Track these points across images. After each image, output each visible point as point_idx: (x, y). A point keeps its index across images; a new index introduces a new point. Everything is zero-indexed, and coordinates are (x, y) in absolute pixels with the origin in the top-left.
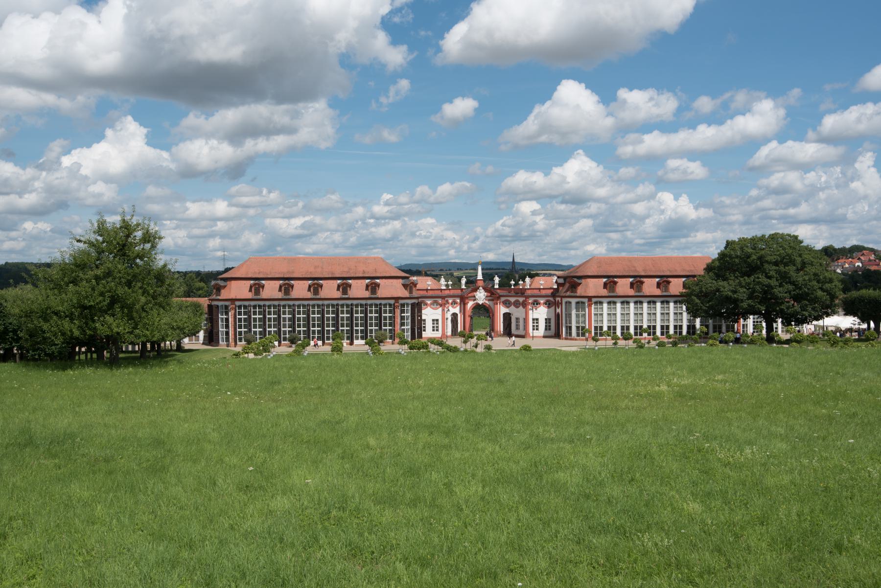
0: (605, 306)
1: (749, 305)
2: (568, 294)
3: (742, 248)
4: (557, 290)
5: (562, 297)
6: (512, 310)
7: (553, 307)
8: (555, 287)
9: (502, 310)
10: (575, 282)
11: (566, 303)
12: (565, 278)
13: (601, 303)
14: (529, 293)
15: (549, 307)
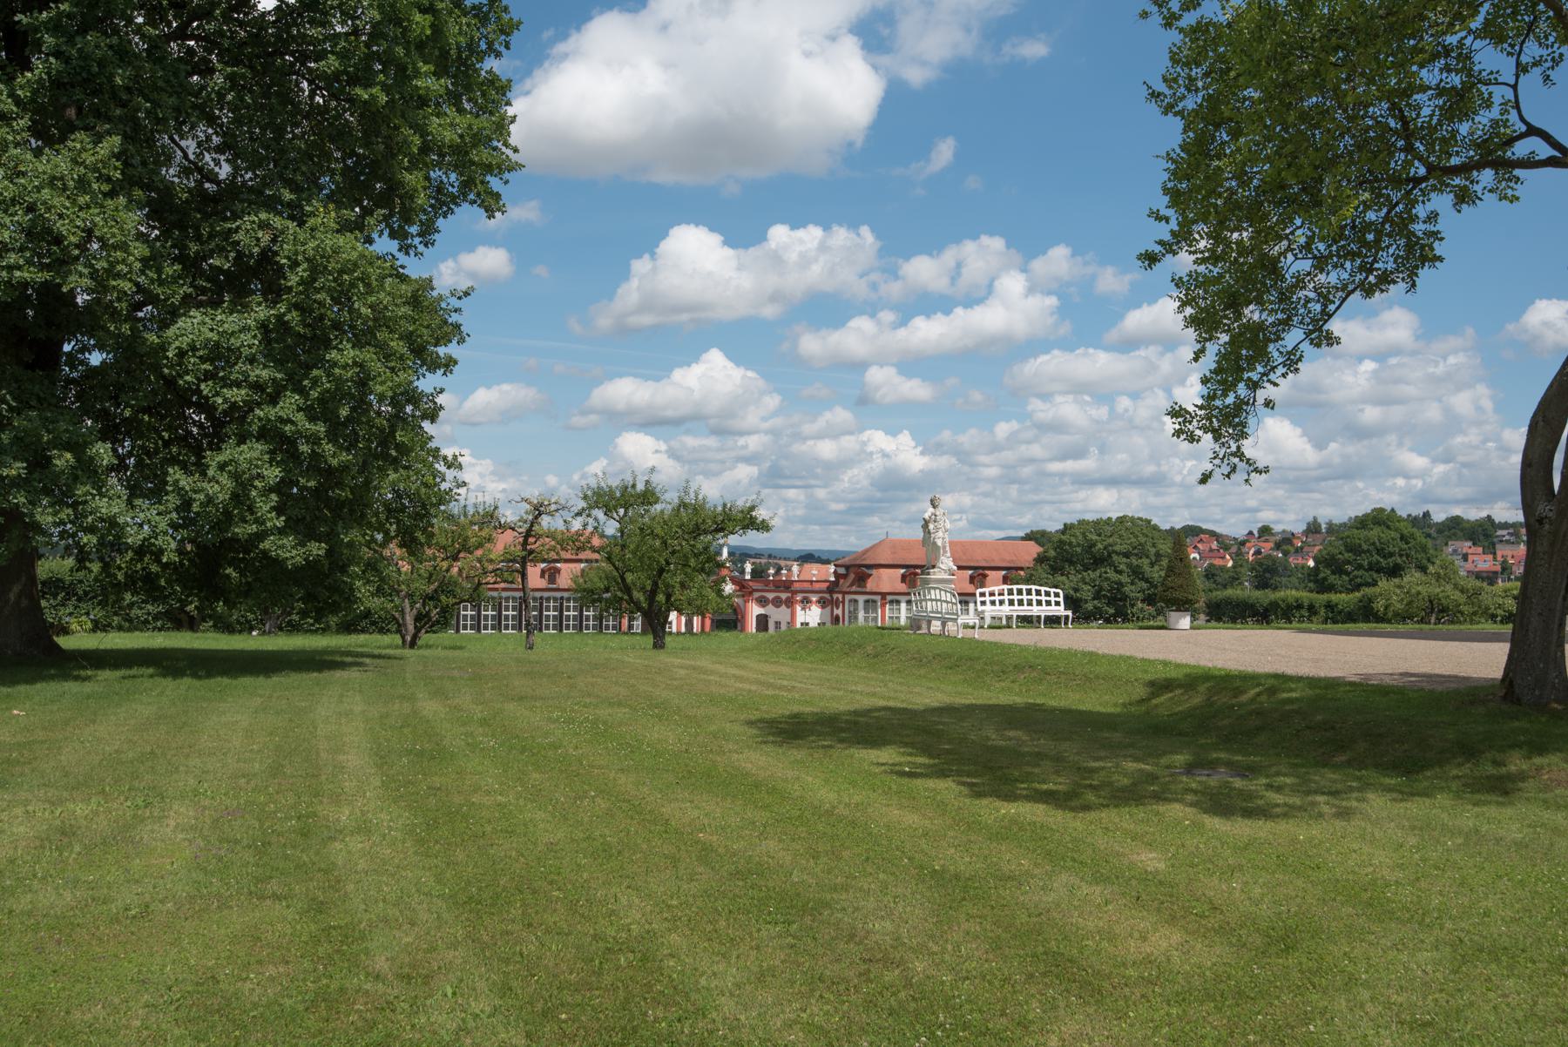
0: (903, 606)
1: (1095, 607)
2: (854, 588)
3: (1084, 534)
4: (836, 583)
5: (844, 593)
6: (770, 610)
7: (828, 609)
8: (833, 579)
9: (755, 610)
10: (864, 573)
11: (850, 601)
12: (847, 567)
13: (898, 602)
14: (797, 586)
15: (823, 607)
